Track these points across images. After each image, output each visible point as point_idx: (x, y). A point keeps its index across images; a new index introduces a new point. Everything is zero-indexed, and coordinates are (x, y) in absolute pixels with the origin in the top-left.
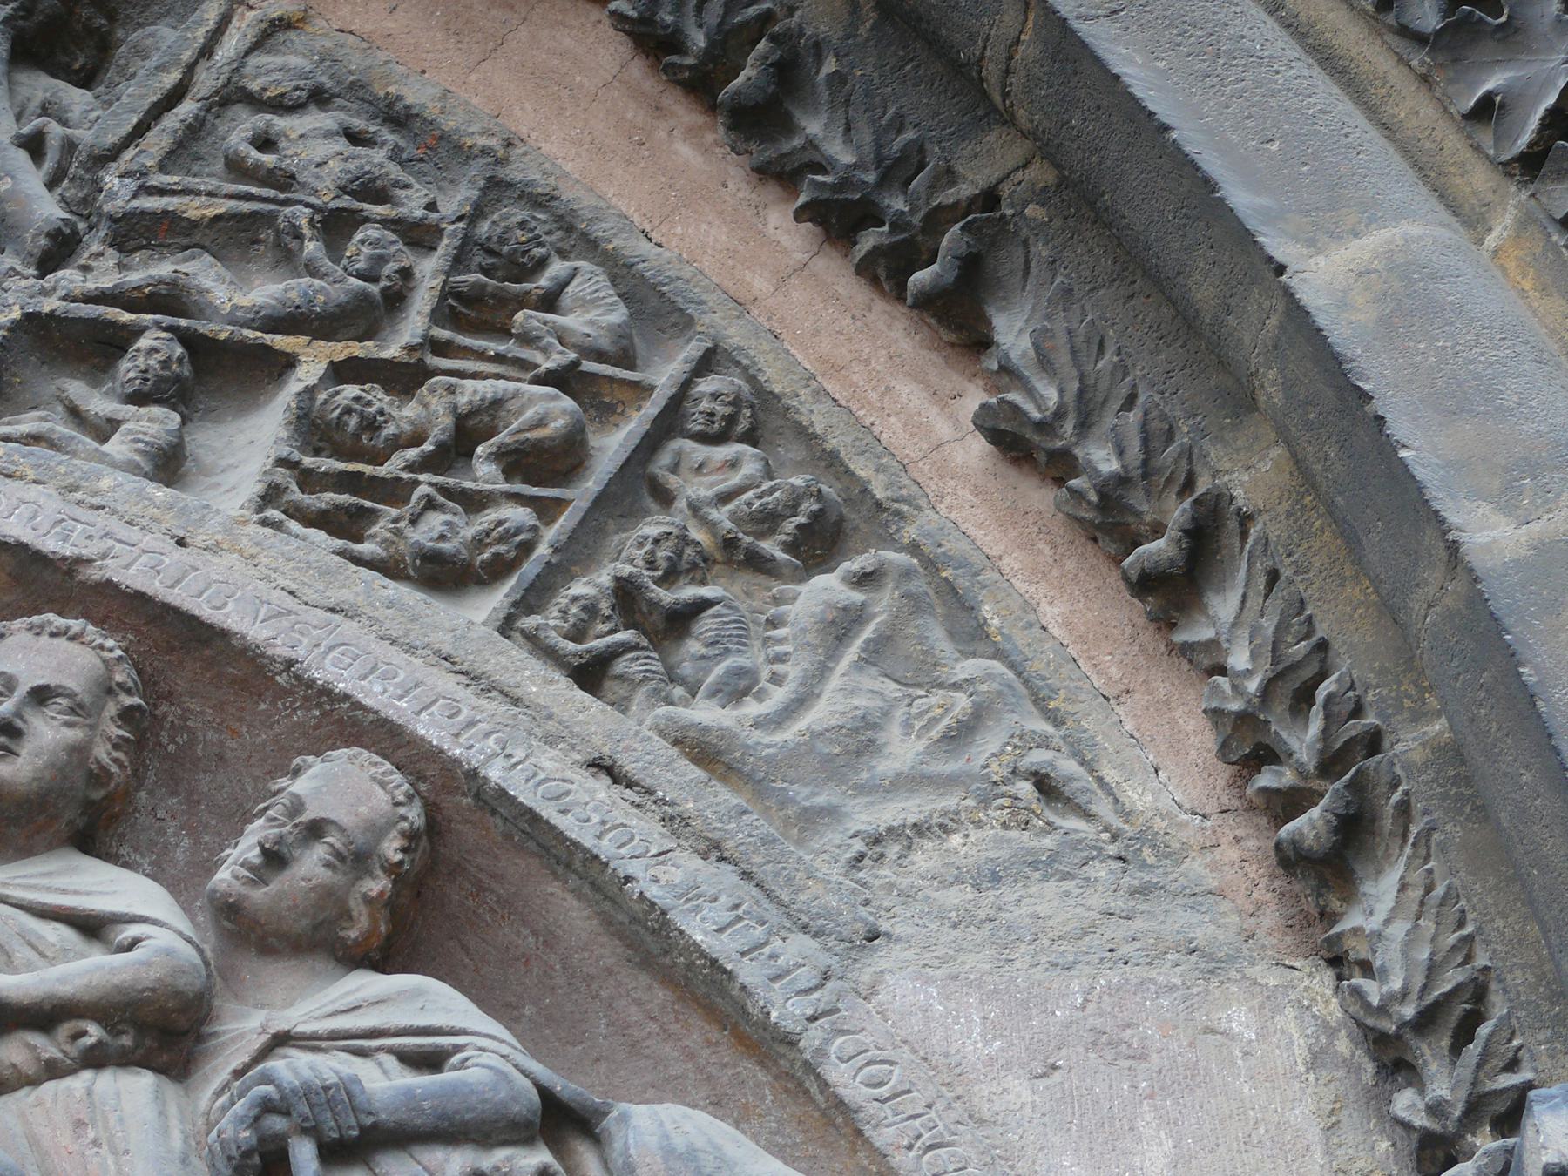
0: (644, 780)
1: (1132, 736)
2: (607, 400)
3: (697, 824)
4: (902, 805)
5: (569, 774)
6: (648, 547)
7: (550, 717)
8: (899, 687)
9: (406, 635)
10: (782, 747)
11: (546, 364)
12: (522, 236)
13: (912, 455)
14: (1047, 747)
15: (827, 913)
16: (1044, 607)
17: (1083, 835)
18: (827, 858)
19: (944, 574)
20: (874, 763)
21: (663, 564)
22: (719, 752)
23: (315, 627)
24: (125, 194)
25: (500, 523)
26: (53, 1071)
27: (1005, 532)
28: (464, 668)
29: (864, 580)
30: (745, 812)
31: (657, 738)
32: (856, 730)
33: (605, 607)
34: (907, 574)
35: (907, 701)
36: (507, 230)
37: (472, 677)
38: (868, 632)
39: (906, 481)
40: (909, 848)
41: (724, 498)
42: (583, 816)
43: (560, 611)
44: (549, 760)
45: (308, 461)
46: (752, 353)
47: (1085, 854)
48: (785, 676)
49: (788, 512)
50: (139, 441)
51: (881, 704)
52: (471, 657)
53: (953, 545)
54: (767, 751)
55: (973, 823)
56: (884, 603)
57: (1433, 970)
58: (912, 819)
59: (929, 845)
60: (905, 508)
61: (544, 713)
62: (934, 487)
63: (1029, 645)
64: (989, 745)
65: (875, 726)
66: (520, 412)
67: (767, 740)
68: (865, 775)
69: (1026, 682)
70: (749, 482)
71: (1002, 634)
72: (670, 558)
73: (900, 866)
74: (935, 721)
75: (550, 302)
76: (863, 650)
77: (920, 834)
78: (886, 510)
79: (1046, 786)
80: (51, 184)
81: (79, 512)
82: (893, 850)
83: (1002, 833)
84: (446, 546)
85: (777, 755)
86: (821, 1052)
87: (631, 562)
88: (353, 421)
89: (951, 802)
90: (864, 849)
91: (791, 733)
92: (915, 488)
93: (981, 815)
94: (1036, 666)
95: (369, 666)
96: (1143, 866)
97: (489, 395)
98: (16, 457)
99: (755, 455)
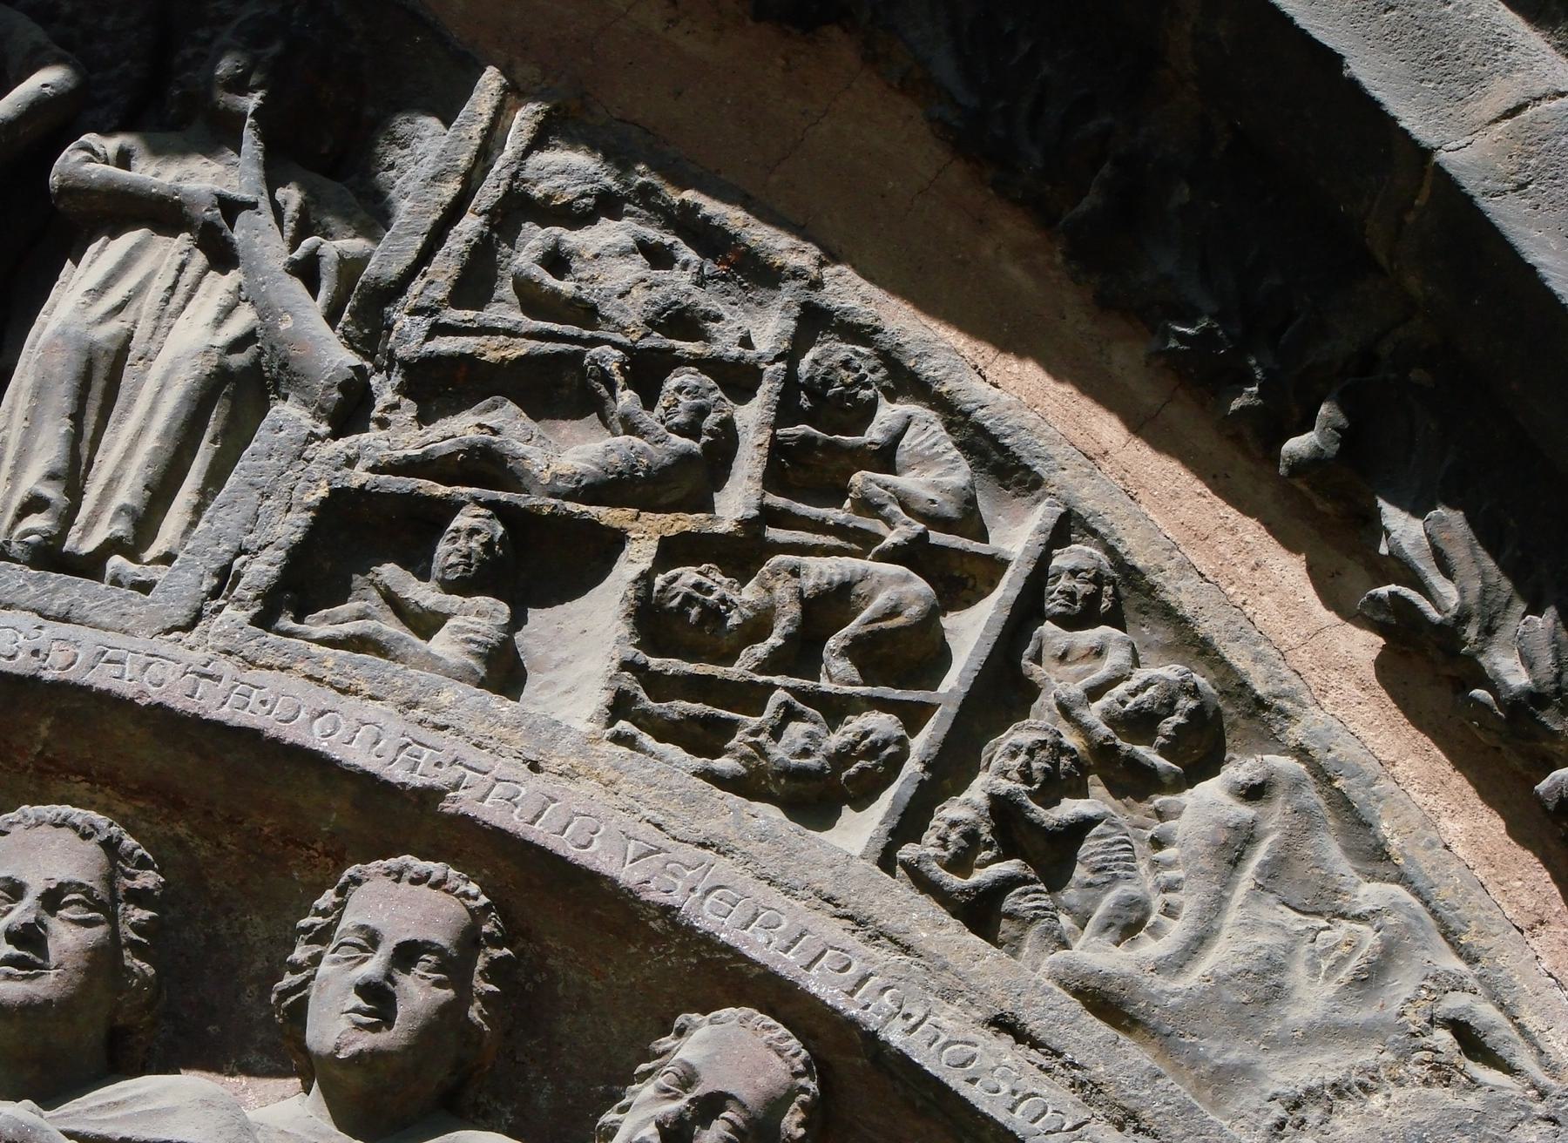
0: (1050, 1040)
1: (1550, 975)
2: (957, 574)
3: (1111, 1090)
4: (1317, 1060)
5: (971, 1036)
6: (1022, 758)
7: (944, 967)
8: (1299, 916)
9: (784, 870)
10: (1187, 996)
11: (892, 538)
12: (849, 376)
13: (1290, 641)
14: (1464, 990)
16: (1445, 822)
17: (1510, 1093)
18: (1245, 1124)
19: (1336, 784)
20: (1283, 1012)
21: (1039, 777)
22: (1122, 1003)
23: (688, 868)
25: (866, 734)
27: (1397, 734)
28: (849, 911)
29: (1254, 793)
30: (1159, 1076)
31: (1058, 989)
32: (1261, 975)
33: (985, 831)
34: (1297, 785)
35: (1311, 935)
36: (831, 369)
37: (858, 922)
38: (1260, 854)
39: (1287, 673)
40: (1330, 1111)
41: (1094, 693)
42: (994, 1087)
43: (939, 838)
44: (949, 1018)
45: (655, 663)
46: (1108, 518)
47: (1513, 1115)
48: (1179, 907)
49: (1164, 711)
50: (471, 641)
51: (1284, 940)
52: (855, 898)
53: (1345, 750)
54: (1172, 1001)
55: (1393, 1080)
56: (1276, 818)
58: (1331, 1078)
59: (1350, 1107)
60: (1288, 705)
61: (938, 963)
62: (1317, 680)
63: (1433, 868)
64: (1402, 987)
65: (1281, 968)
66: (869, 598)
67: (1172, 986)
68: (1276, 1026)
69: (1434, 912)
70: (1119, 674)
71: (1403, 855)
72: (1045, 771)
73: (1323, 1132)
74: (1342, 960)
75: (885, 458)
76: (1259, 875)
77: (1340, 1095)
78: (1268, 708)
80: (332, 317)
81: (424, 734)
82: (1313, 1114)
83: (1424, 1090)
84: (812, 762)
85: (1182, 1005)
87: (1004, 774)
88: (694, 612)
89: (1368, 1056)
90: (1284, 1115)
91: (1193, 979)
92: (1296, 681)
93: (1401, 1071)
94: (1444, 894)
95: (750, 913)
97: (837, 578)
98: (348, 669)
99: (1121, 640)
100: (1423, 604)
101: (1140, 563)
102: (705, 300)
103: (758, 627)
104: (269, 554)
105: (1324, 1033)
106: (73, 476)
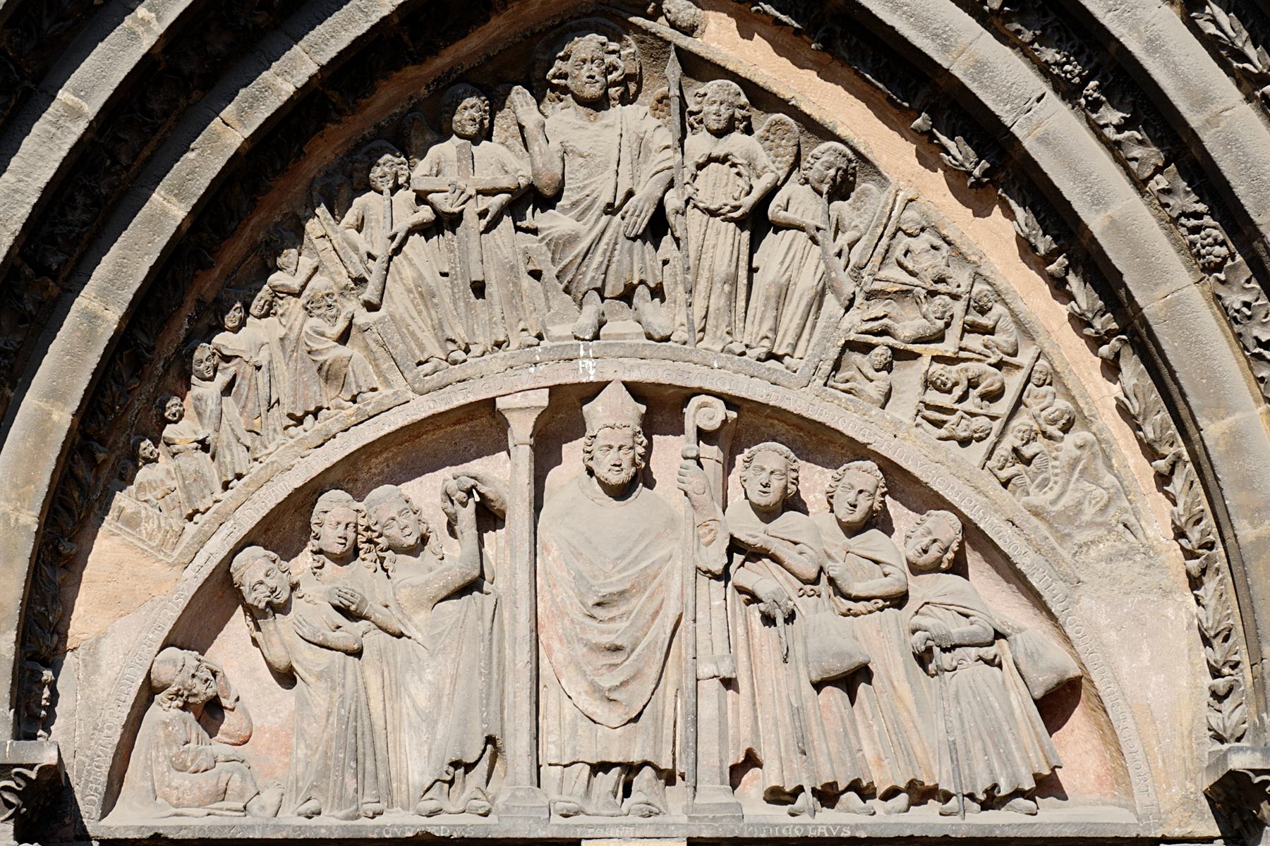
6: (1021, 434)
11: (993, 360)
12: (985, 299)
15: (1067, 575)
24: (870, 282)
26: (870, 612)
38: (1080, 467)
57: (1219, 622)
58: (1090, 539)
74: (1098, 502)
79: (1125, 525)
81: (868, 424)
82: (1085, 549)
86: (1065, 623)
88: (939, 382)
91: (1059, 507)
94: (1125, 483)
96: (1150, 557)
100: (1130, 407)
101: (1059, 370)
102: (949, 272)
103: (956, 384)
104: (827, 362)
105: (1091, 524)
106: (775, 330)
